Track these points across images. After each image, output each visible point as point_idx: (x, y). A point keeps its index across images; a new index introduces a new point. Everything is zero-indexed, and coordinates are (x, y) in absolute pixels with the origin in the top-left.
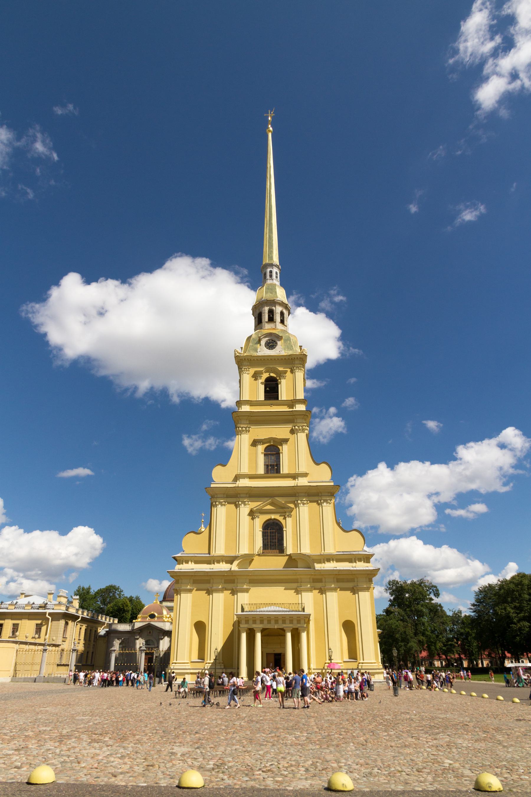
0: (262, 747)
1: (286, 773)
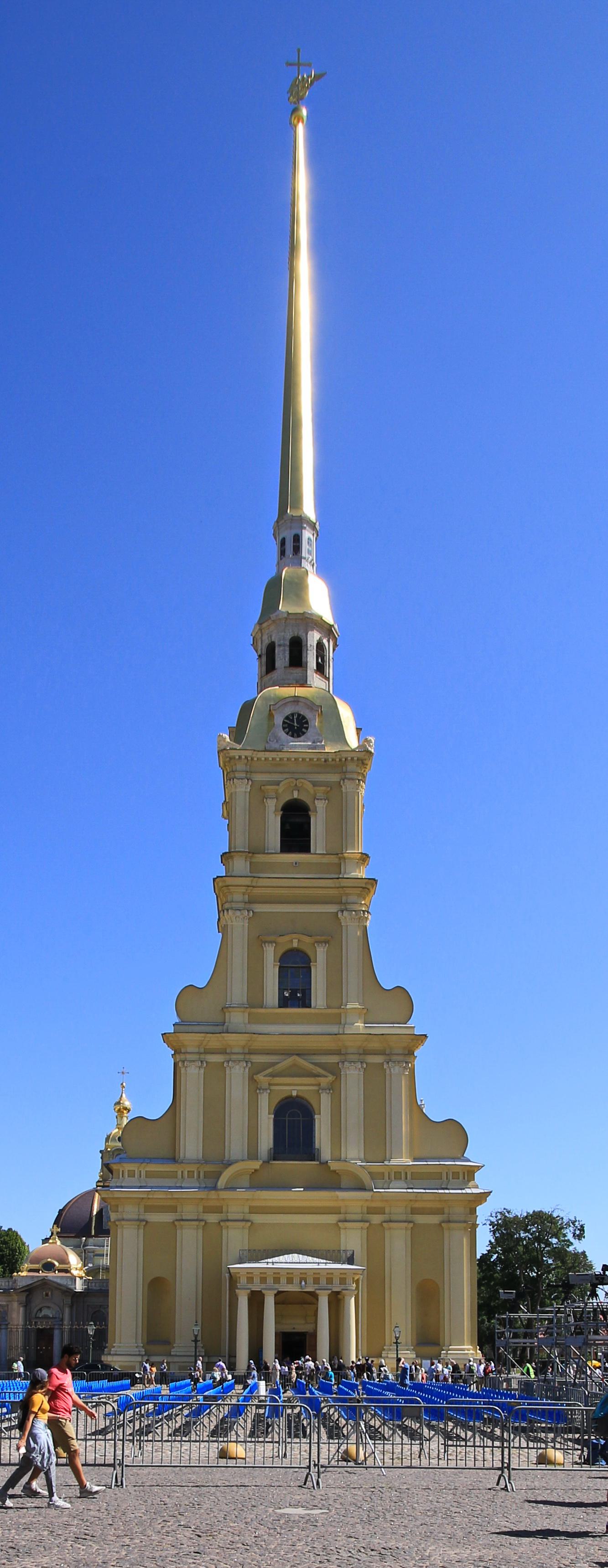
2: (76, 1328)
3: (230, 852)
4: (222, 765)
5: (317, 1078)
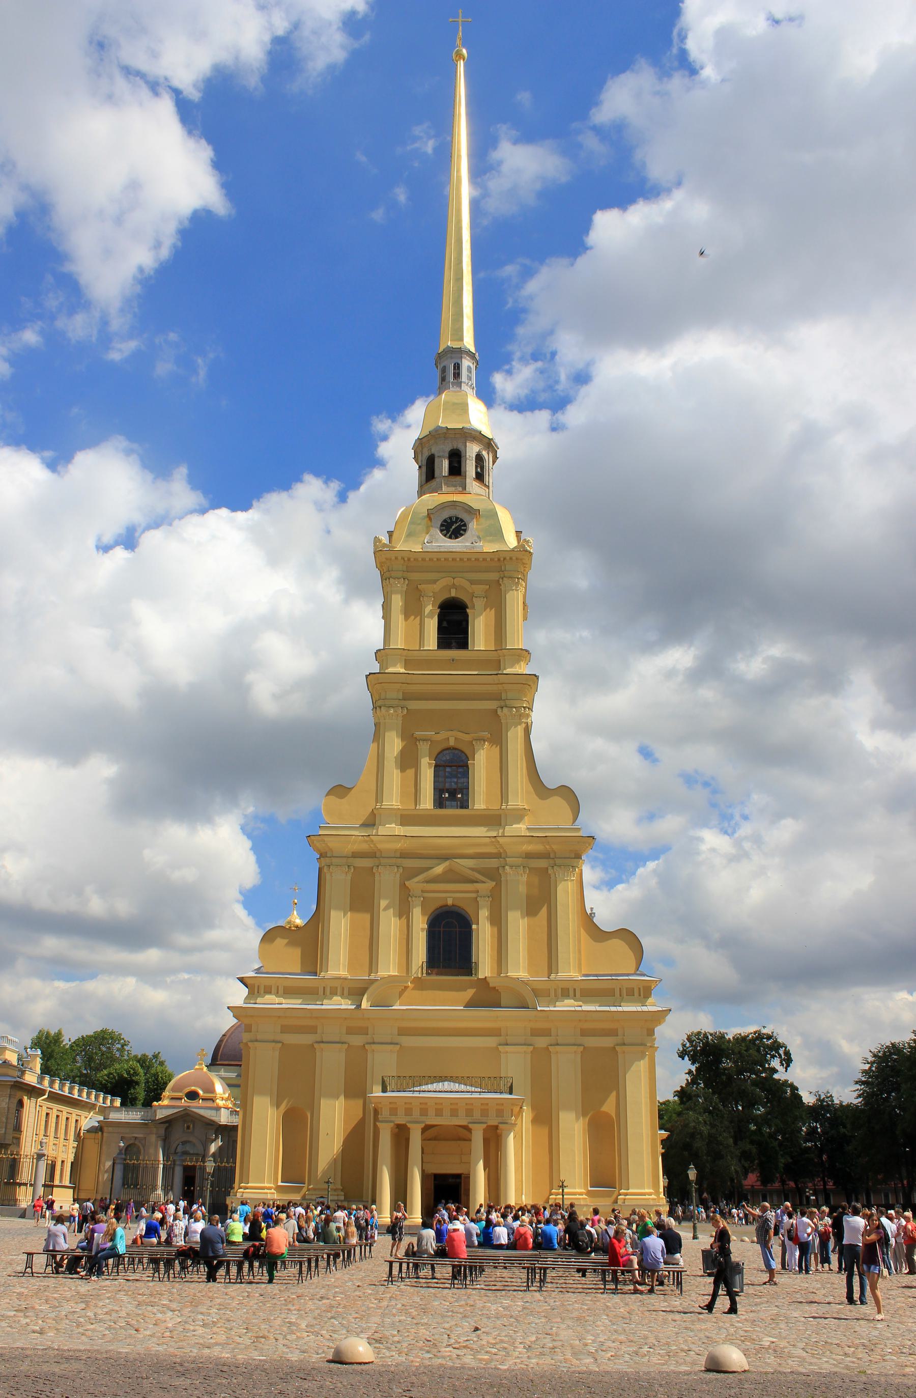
1: (494, 1350)
2: (200, 1165)
3: (384, 649)
4: (378, 566)
5: (475, 884)
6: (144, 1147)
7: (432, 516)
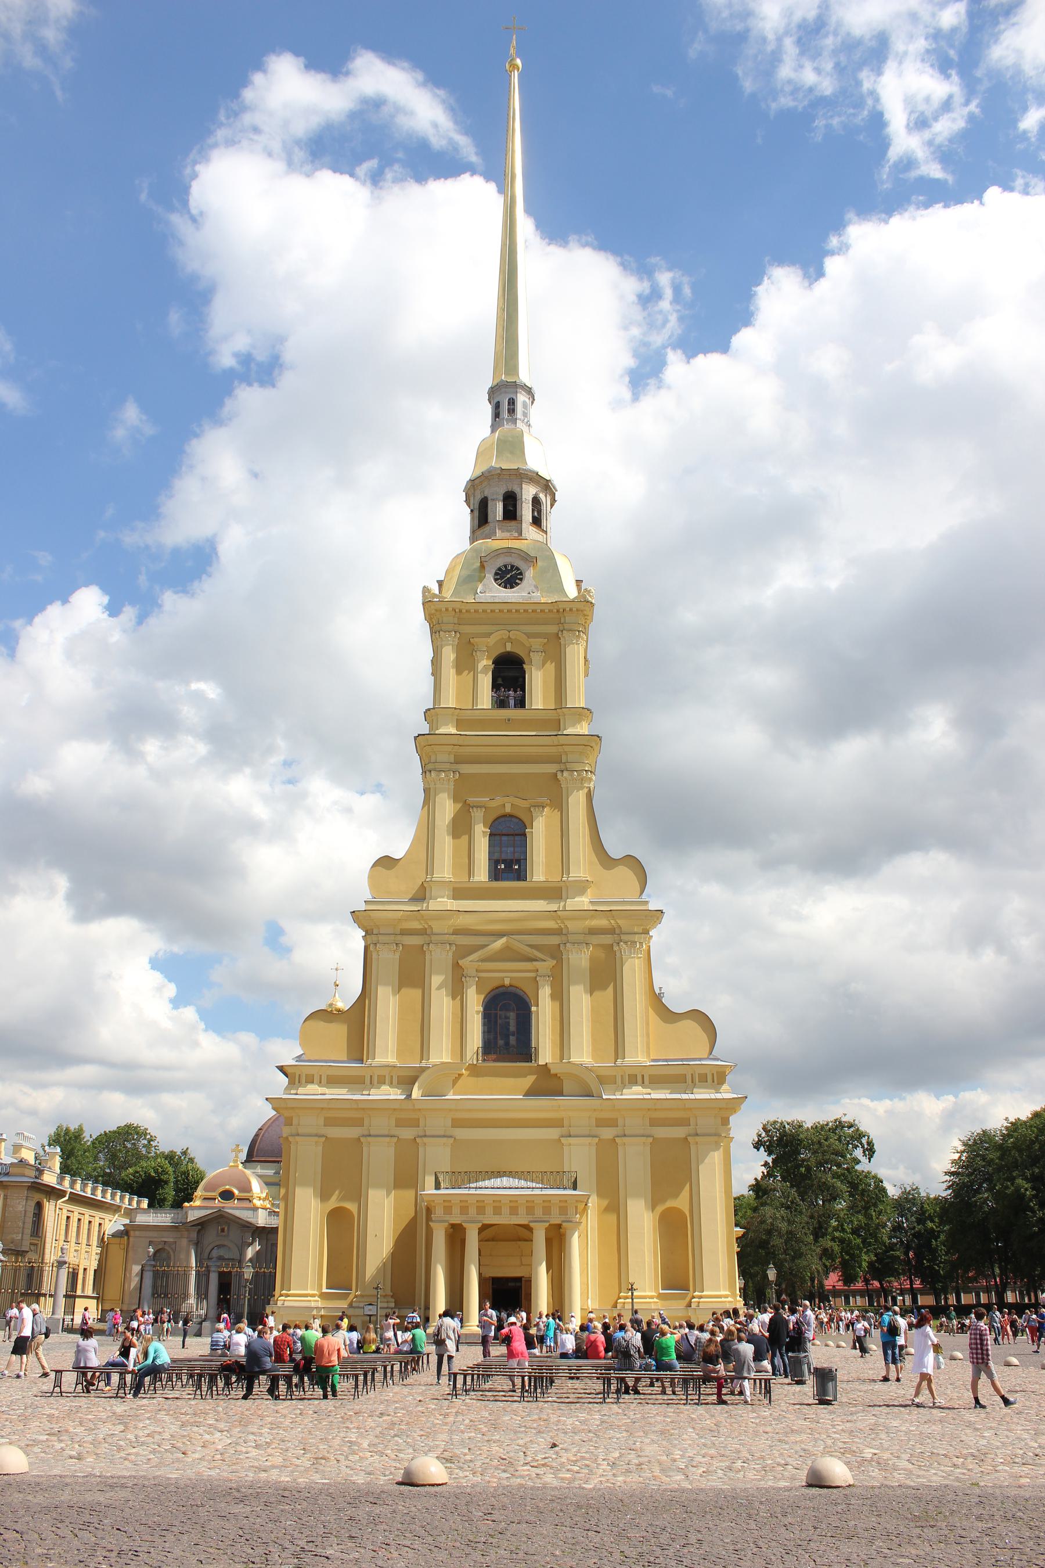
0: (519, 1435)
3: (434, 708)
5: (535, 963)
6: (174, 1252)
7: (485, 564)
